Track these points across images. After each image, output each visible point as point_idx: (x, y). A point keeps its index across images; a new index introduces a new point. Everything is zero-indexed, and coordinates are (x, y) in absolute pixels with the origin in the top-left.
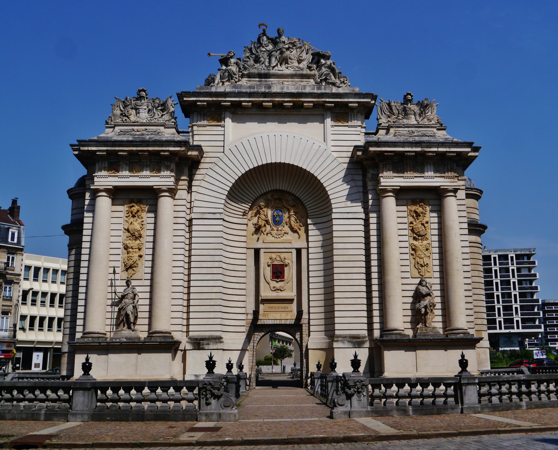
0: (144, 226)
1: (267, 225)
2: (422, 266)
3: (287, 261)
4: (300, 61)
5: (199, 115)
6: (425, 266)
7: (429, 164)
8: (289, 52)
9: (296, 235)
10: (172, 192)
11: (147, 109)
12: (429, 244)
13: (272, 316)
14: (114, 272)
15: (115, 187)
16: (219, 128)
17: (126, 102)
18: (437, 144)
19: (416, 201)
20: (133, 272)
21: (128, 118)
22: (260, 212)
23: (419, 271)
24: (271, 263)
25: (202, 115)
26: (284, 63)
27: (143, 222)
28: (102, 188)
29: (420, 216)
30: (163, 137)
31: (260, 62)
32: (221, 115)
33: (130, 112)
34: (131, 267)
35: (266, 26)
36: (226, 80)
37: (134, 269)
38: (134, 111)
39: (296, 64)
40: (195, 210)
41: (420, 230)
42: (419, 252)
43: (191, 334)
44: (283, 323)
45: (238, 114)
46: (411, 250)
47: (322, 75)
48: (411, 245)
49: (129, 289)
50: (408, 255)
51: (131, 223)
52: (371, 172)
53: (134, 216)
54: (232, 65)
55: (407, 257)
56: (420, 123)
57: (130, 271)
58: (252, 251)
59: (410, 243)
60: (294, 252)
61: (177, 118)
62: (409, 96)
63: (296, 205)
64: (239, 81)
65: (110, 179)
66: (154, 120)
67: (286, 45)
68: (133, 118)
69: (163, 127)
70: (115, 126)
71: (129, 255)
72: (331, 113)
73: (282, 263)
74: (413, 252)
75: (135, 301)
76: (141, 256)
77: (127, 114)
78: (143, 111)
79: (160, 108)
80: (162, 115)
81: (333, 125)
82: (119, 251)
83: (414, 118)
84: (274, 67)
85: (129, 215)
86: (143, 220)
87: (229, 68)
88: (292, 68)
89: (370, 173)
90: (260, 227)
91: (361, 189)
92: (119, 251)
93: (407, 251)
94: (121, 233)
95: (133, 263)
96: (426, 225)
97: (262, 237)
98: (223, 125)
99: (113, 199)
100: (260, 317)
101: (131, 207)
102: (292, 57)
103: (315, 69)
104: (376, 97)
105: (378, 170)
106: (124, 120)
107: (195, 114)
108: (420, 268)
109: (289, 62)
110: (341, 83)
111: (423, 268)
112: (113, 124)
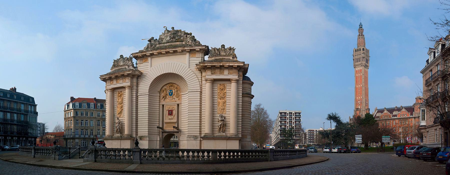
16: (147, 63)
40: (139, 92)
72: (189, 53)
76: (122, 110)
101: (119, 94)
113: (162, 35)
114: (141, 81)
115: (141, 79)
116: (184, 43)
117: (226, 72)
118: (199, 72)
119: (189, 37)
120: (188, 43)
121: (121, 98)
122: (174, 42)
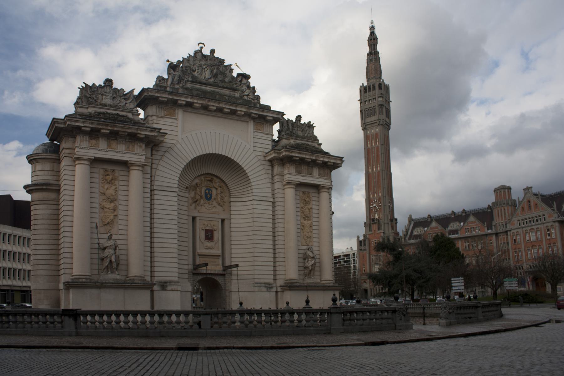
2: (308, 238)
14: (97, 227)
22: (196, 188)
28: (85, 157)
29: (307, 203)
33: (97, 97)
34: (108, 224)
37: (110, 225)
40: (156, 183)
42: (306, 229)
48: (301, 223)
51: (107, 189)
53: (108, 183)
65: (91, 151)
71: (106, 214)
74: (303, 228)
76: (116, 216)
80: (126, 103)
82: (97, 210)
85: (105, 182)
91: (271, 180)
92: (97, 210)
94: (97, 195)
95: (110, 221)
96: (311, 210)
99: (90, 167)
114: (159, 157)
116: (237, 95)
118: (268, 163)
121: (114, 187)
122: (220, 87)
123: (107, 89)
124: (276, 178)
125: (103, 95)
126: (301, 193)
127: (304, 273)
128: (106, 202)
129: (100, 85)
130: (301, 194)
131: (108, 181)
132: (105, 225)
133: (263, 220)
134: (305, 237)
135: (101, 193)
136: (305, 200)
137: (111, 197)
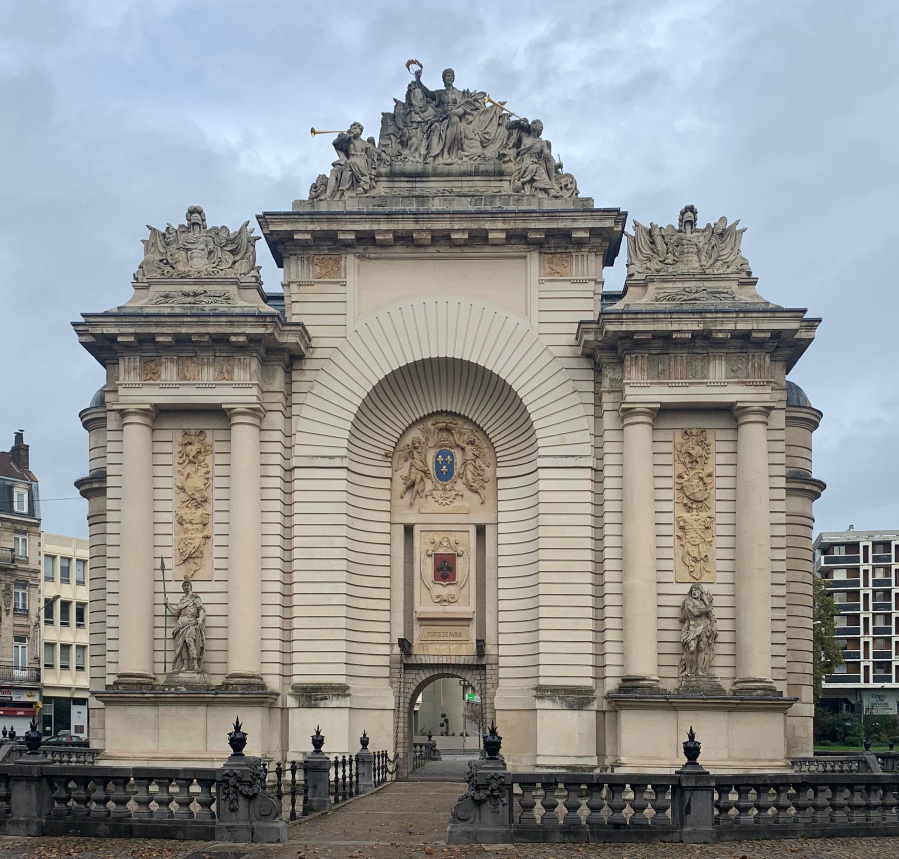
0: (210, 481)
1: (426, 479)
3: (460, 549)
4: (484, 144)
5: (299, 261)
6: (702, 561)
7: (717, 358)
8: (464, 123)
9: (477, 496)
10: (257, 413)
11: (206, 250)
12: (710, 518)
13: (434, 649)
15: (155, 406)
17: (168, 236)
18: (734, 315)
19: (691, 433)
20: (195, 567)
21: (173, 268)
23: (692, 569)
24: (433, 551)
25: (305, 262)
26: (455, 149)
27: (207, 473)
30: (235, 307)
31: (412, 145)
32: (337, 262)
33: (177, 256)
34: (190, 557)
35: (421, 66)
36: (348, 186)
37: (196, 560)
38: (183, 253)
39: (479, 150)
40: (297, 450)
41: (696, 491)
42: (691, 534)
43: (296, 680)
44: (453, 662)
45: (370, 259)
46: (677, 529)
47: (525, 172)
48: (679, 519)
49: (188, 598)
50: (671, 539)
52: (609, 374)
53: (190, 462)
54: (359, 153)
55: (669, 542)
56: (707, 271)
57: (191, 566)
58: (401, 530)
59: (677, 516)
60: (473, 530)
61: (260, 267)
62: (689, 213)
63: (477, 441)
64: (372, 188)
66: (220, 271)
67: (459, 107)
68: (181, 267)
69: (235, 287)
70: (150, 284)
71: (186, 536)
73: (452, 552)
74: (680, 534)
75: (200, 620)
76: (207, 538)
77: (170, 261)
78: (200, 255)
79: (228, 249)
80: (234, 262)
81: (542, 280)
82: (168, 529)
83: (697, 259)
84: (435, 157)
85: (184, 461)
86: (208, 469)
87: (353, 159)
88: (470, 159)
89: (609, 377)
90: (413, 485)
91: (591, 410)
92: (168, 529)
93: (668, 530)
97: (419, 501)
98: (343, 282)
99: (153, 430)
100: (416, 650)
102: (471, 135)
103: (512, 159)
104: (623, 217)
105: (623, 371)
106: (165, 272)
107: (293, 258)
108: (693, 564)
109: (465, 146)
110: (561, 188)
111: (698, 564)
112: (146, 281)
113: (393, 117)
114: (304, 387)
115: (309, 376)
116: (506, 187)
117: (718, 370)
118: (584, 363)
119: (529, 149)
120: (527, 187)
121: (202, 471)
123: (194, 234)
124: (608, 400)
125: (187, 250)
126: (679, 434)
127: (682, 660)
128: (187, 507)
129: (181, 226)
130: (679, 438)
131: (191, 457)
132: (185, 561)
133: (565, 520)
134: (688, 560)
135: (178, 487)
136: (690, 455)
137: (197, 495)
